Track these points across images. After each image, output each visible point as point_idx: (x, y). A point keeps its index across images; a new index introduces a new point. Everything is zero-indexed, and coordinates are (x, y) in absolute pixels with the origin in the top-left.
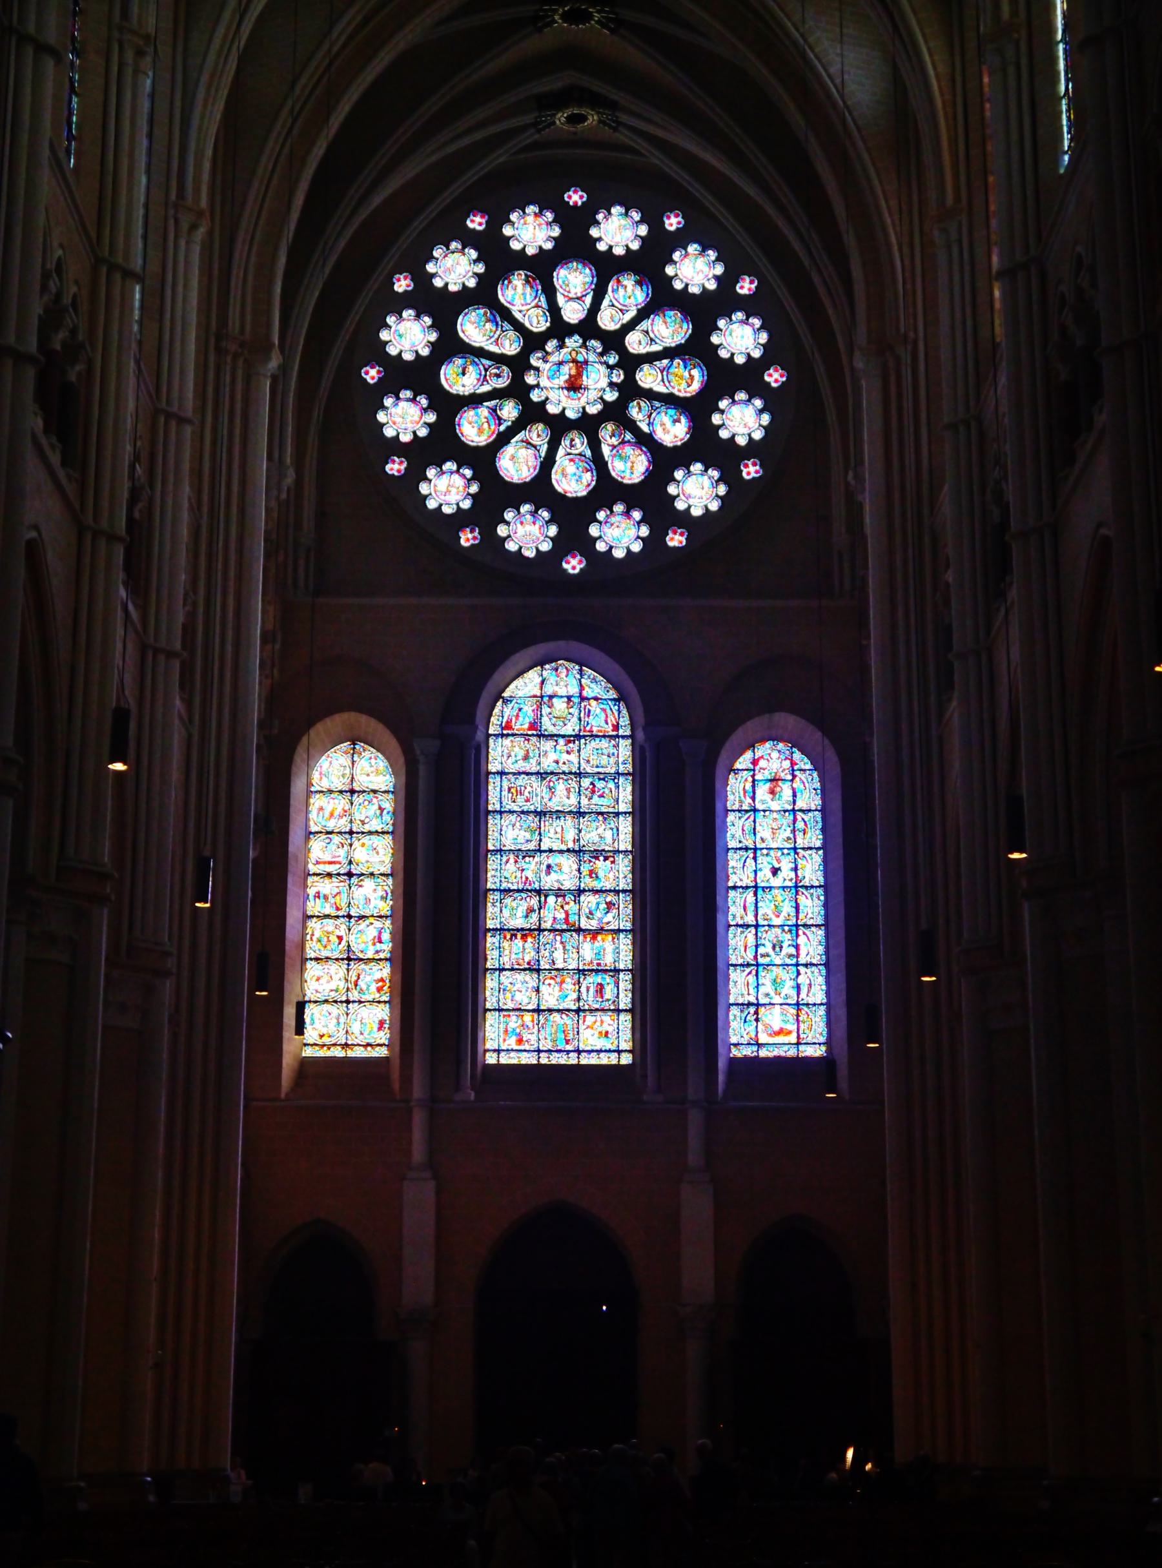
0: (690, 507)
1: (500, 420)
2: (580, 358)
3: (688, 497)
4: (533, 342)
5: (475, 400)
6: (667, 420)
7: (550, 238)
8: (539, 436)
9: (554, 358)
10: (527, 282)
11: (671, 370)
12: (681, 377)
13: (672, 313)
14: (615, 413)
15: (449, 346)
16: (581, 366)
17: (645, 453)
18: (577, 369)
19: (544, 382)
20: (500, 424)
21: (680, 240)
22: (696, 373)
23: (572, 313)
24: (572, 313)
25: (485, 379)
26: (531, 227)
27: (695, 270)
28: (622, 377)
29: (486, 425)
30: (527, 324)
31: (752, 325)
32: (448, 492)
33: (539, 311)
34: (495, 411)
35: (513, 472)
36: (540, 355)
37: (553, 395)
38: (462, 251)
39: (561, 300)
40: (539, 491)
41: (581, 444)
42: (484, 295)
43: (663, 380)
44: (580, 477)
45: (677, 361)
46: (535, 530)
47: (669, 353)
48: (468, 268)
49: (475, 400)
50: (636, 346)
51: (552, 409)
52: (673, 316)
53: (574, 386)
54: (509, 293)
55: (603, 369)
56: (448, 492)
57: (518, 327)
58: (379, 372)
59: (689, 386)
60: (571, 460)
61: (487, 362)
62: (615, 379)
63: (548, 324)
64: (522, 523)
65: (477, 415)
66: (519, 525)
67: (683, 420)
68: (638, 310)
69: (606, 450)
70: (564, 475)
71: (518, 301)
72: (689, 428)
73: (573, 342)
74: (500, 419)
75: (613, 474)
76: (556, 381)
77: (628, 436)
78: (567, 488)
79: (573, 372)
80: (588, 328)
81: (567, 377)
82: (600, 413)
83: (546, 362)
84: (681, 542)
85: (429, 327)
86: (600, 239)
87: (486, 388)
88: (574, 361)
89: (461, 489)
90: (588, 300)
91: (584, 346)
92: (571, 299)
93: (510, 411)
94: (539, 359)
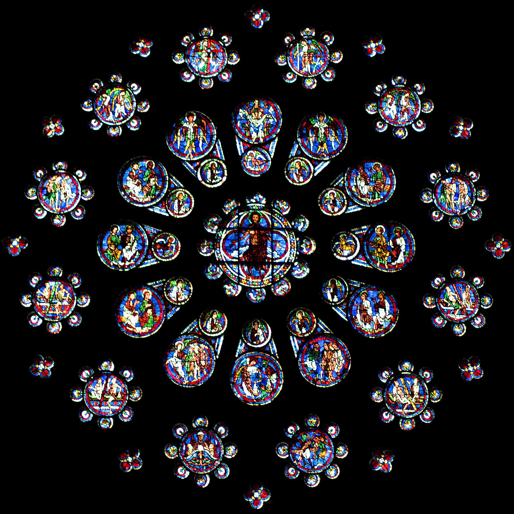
0: (397, 418)
1: (168, 305)
2: (264, 224)
3: (396, 405)
4: (208, 203)
5: (137, 278)
6: (367, 303)
7: (228, 68)
8: (213, 326)
9: (233, 224)
10: (200, 125)
11: (372, 239)
12: (386, 248)
13: (372, 165)
14: (306, 295)
15: (108, 208)
16: (265, 234)
17: (342, 349)
18: (260, 236)
19: (221, 255)
20: (167, 311)
21: (382, 70)
22: (401, 242)
23: (255, 164)
24: (255, 164)
25: (149, 252)
26: (204, 56)
27: (399, 110)
28: (314, 248)
29: (149, 311)
30: (200, 178)
31: (468, 180)
32: (103, 401)
33: (215, 162)
34: (161, 293)
35: (182, 373)
36: (215, 220)
37: (233, 271)
38: (124, 86)
39: (240, 147)
40: (215, 397)
41: (264, 335)
42: (151, 141)
43: (361, 251)
44: (264, 381)
45: (379, 228)
46: (209, 450)
47: (369, 216)
48: (129, 107)
49: (137, 278)
50: (329, 208)
51: (230, 290)
52: (376, 167)
53: (256, 260)
54: (179, 138)
55: (291, 238)
56: (103, 401)
57: (190, 183)
58: (21, 243)
59: (394, 259)
60: (252, 358)
61: (152, 230)
62: (305, 251)
63: (225, 179)
64: (193, 443)
65: (139, 298)
66: (190, 446)
67: (387, 305)
68: (331, 160)
69: (295, 344)
70: (245, 377)
71: (189, 147)
72: (394, 314)
73: (257, 202)
74: (167, 303)
75: (304, 376)
76: (235, 254)
77: (322, 326)
78: (248, 394)
79: (254, 241)
80: (274, 184)
81: (247, 247)
82: (288, 295)
83: (222, 227)
84: (387, 466)
85: (82, 184)
86: (287, 69)
87: (150, 263)
88: (256, 226)
89: (119, 396)
90: (273, 147)
91: (268, 207)
92: (253, 147)
93: (179, 292)
94: (214, 224)
